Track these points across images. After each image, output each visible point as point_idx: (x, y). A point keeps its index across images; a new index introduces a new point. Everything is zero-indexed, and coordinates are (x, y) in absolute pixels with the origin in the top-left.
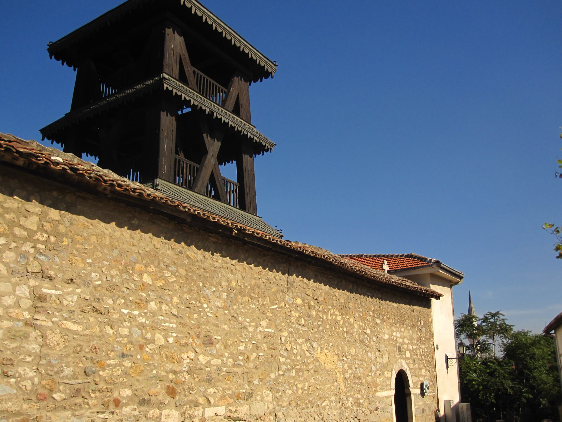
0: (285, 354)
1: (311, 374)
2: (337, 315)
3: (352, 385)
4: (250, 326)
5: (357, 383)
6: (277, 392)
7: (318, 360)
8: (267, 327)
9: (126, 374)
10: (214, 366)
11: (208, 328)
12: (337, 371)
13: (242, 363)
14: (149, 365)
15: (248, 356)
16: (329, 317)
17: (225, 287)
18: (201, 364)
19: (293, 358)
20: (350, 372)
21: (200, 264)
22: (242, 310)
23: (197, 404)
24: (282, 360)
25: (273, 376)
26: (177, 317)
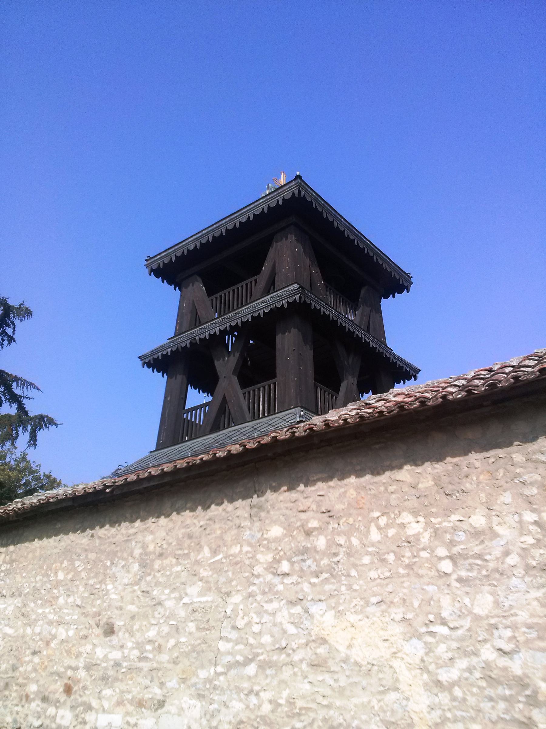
0: (234, 635)
1: (302, 671)
2: (403, 526)
3: (472, 701)
4: (169, 599)
5: (505, 699)
6: (211, 704)
7: (324, 641)
8: (200, 595)
9: (35, 670)
10: (112, 660)
11: (109, 613)
12: (396, 664)
13: (151, 656)
14: (51, 661)
15: (160, 646)
16: (375, 535)
17: (137, 556)
18: (98, 659)
19: (251, 641)
20: (463, 663)
21: (111, 540)
22: (160, 580)
23: (89, 708)
24: (223, 646)
25: (203, 674)
26: (80, 607)
